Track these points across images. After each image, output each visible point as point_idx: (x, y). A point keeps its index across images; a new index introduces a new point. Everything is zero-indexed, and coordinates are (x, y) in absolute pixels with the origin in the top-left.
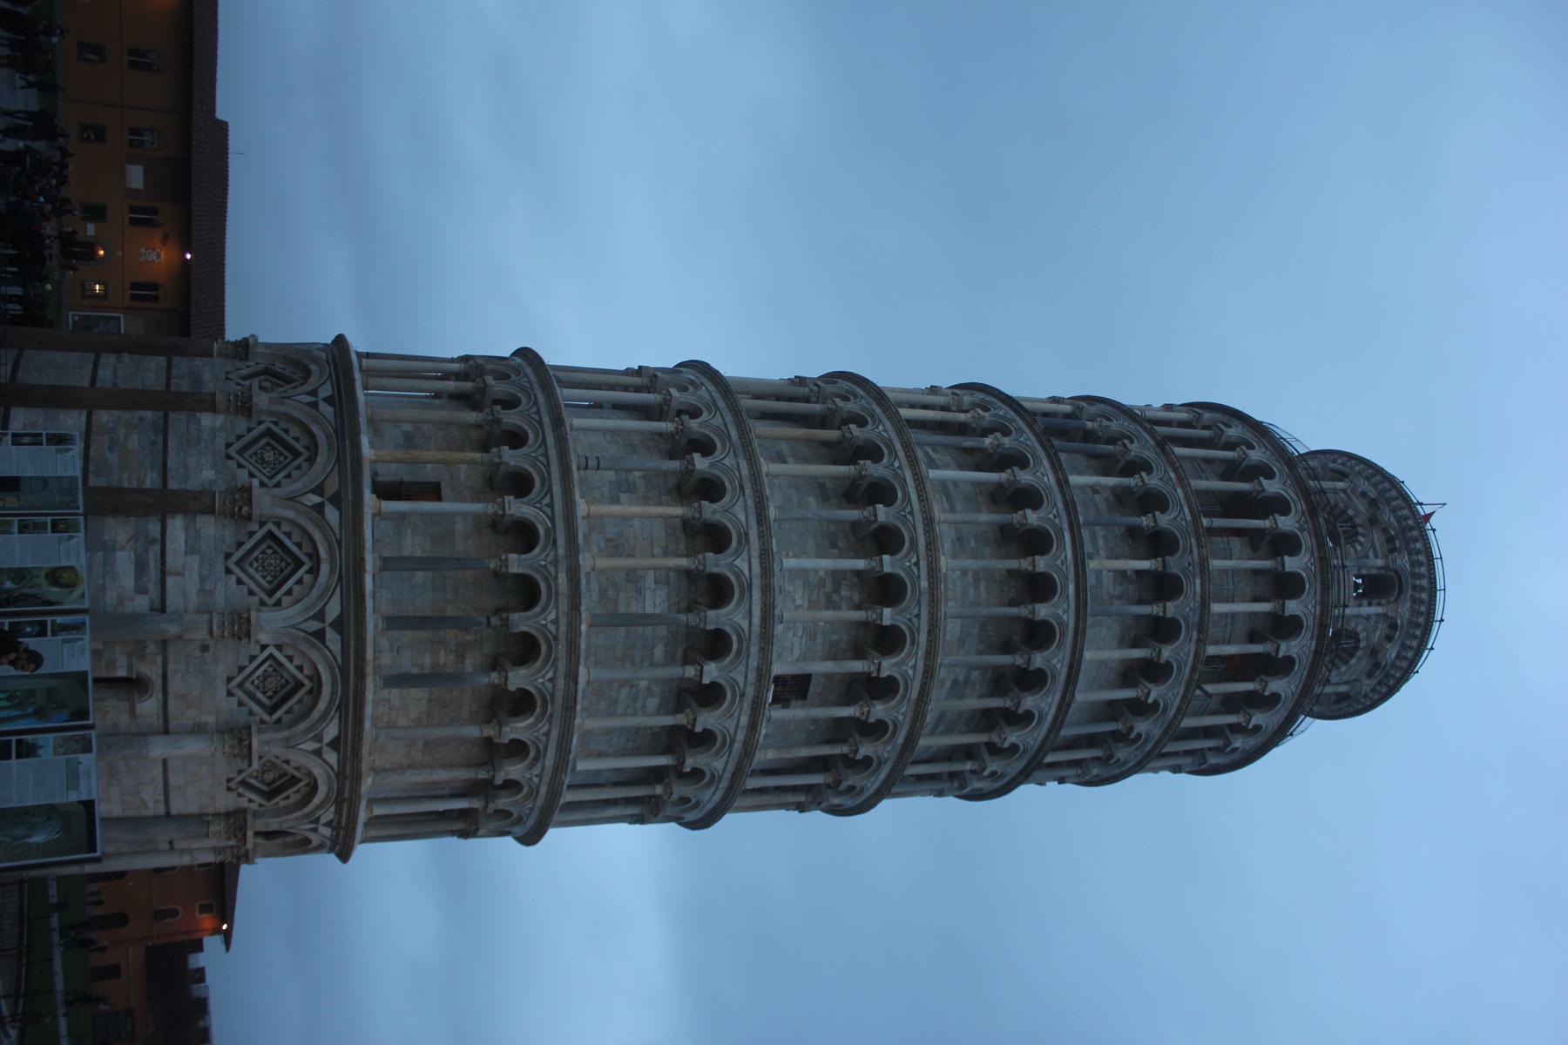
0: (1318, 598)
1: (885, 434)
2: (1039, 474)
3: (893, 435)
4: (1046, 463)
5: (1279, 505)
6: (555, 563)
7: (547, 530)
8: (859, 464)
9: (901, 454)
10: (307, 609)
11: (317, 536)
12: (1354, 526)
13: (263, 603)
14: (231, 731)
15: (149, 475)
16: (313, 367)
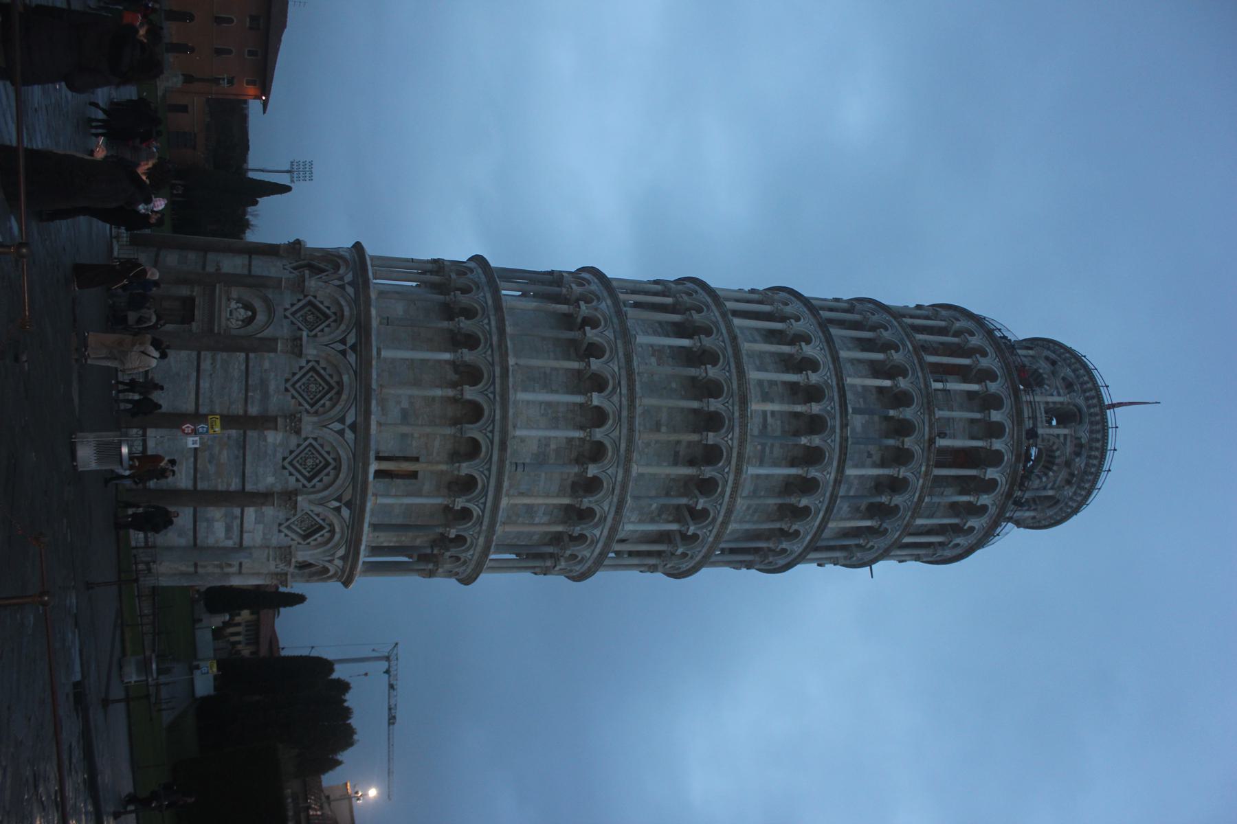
0: (979, 537)
1: (730, 442)
2: (825, 473)
3: (736, 443)
4: (835, 464)
5: (991, 485)
6: (479, 533)
7: (478, 516)
8: (701, 469)
9: (734, 461)
10: (324, 552)
12: (1053, 464)
13: (299, 544)
14: (277, 574)
15: (234, 480)
16: (345, 378)
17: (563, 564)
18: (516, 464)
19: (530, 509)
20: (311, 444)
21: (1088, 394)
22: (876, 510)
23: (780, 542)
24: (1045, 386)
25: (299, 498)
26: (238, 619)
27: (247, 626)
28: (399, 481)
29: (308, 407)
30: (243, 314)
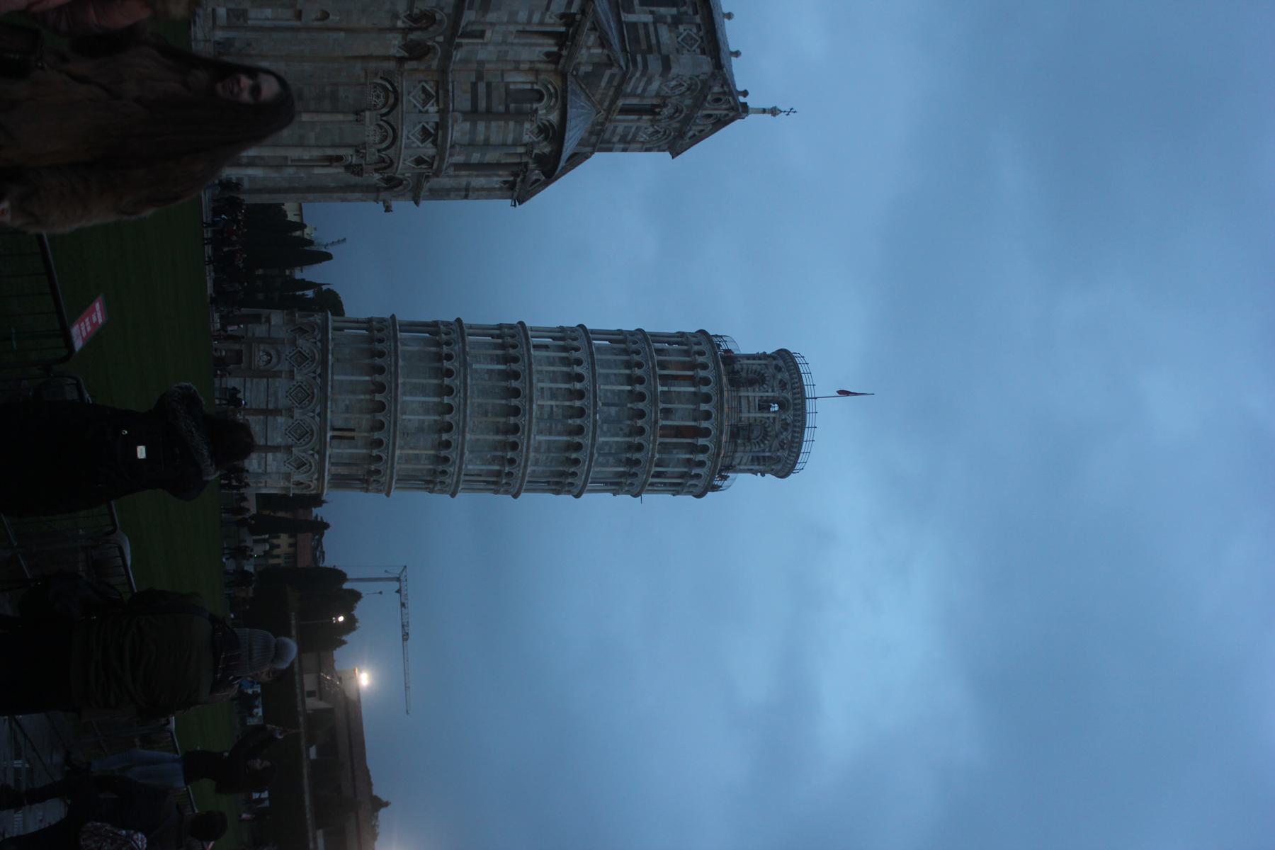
3: (527, 423)
4: (590, 434)
5: (704, 449)
6: (387, 468)
9: (526, 433)
11: (312, 461)
12: (767, 435)
14: (284, 488)
16: (315, 391)
17: (438, 487)
18: (404, 434)
19: (417, 457)
20: (299, 423)
21: (794, 391)
22: (630, 463)
23: (568, 478)
24: (765, 386)
25: (293, 449)
26: (276, 552)
27: (286, 558)
28: (346, 441)
29: (297, 405)
30: (265, 358)
